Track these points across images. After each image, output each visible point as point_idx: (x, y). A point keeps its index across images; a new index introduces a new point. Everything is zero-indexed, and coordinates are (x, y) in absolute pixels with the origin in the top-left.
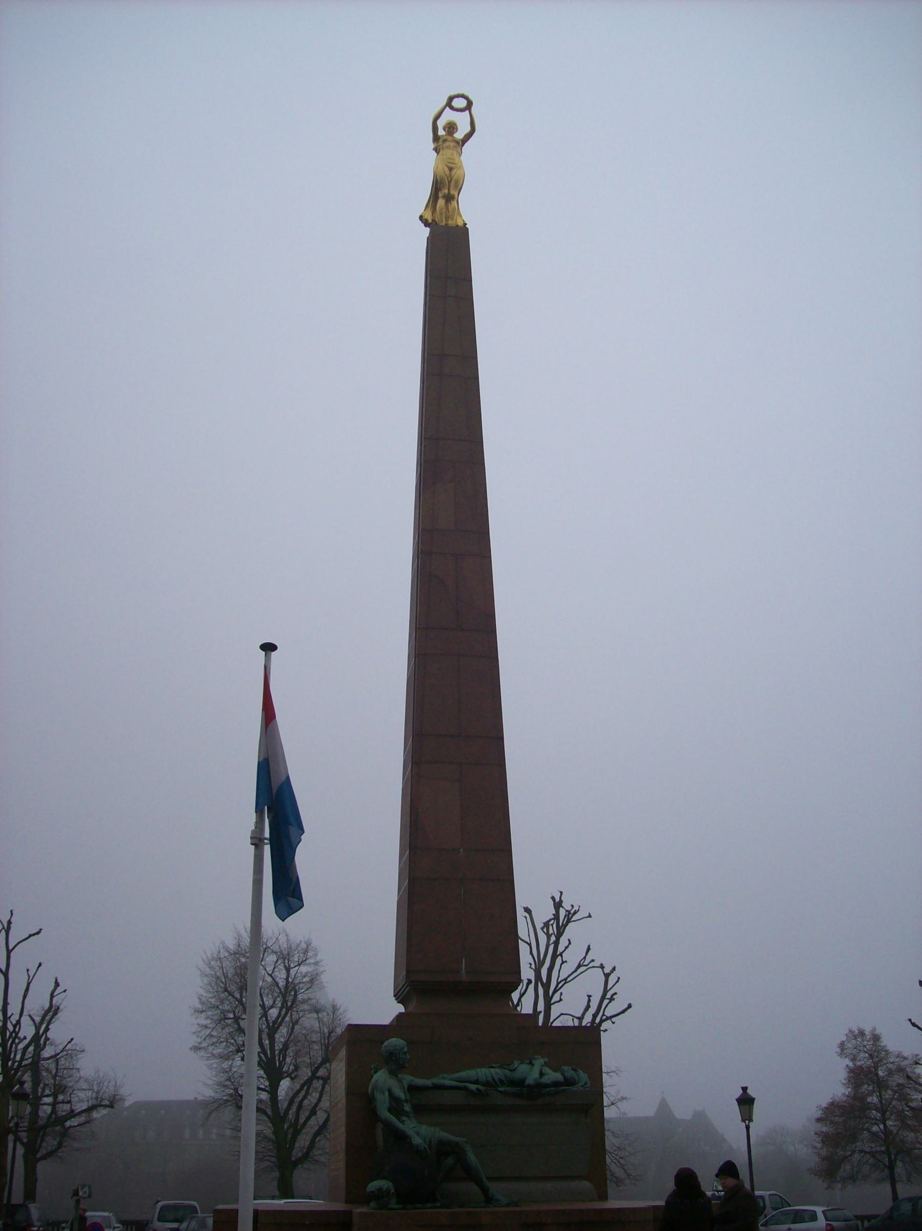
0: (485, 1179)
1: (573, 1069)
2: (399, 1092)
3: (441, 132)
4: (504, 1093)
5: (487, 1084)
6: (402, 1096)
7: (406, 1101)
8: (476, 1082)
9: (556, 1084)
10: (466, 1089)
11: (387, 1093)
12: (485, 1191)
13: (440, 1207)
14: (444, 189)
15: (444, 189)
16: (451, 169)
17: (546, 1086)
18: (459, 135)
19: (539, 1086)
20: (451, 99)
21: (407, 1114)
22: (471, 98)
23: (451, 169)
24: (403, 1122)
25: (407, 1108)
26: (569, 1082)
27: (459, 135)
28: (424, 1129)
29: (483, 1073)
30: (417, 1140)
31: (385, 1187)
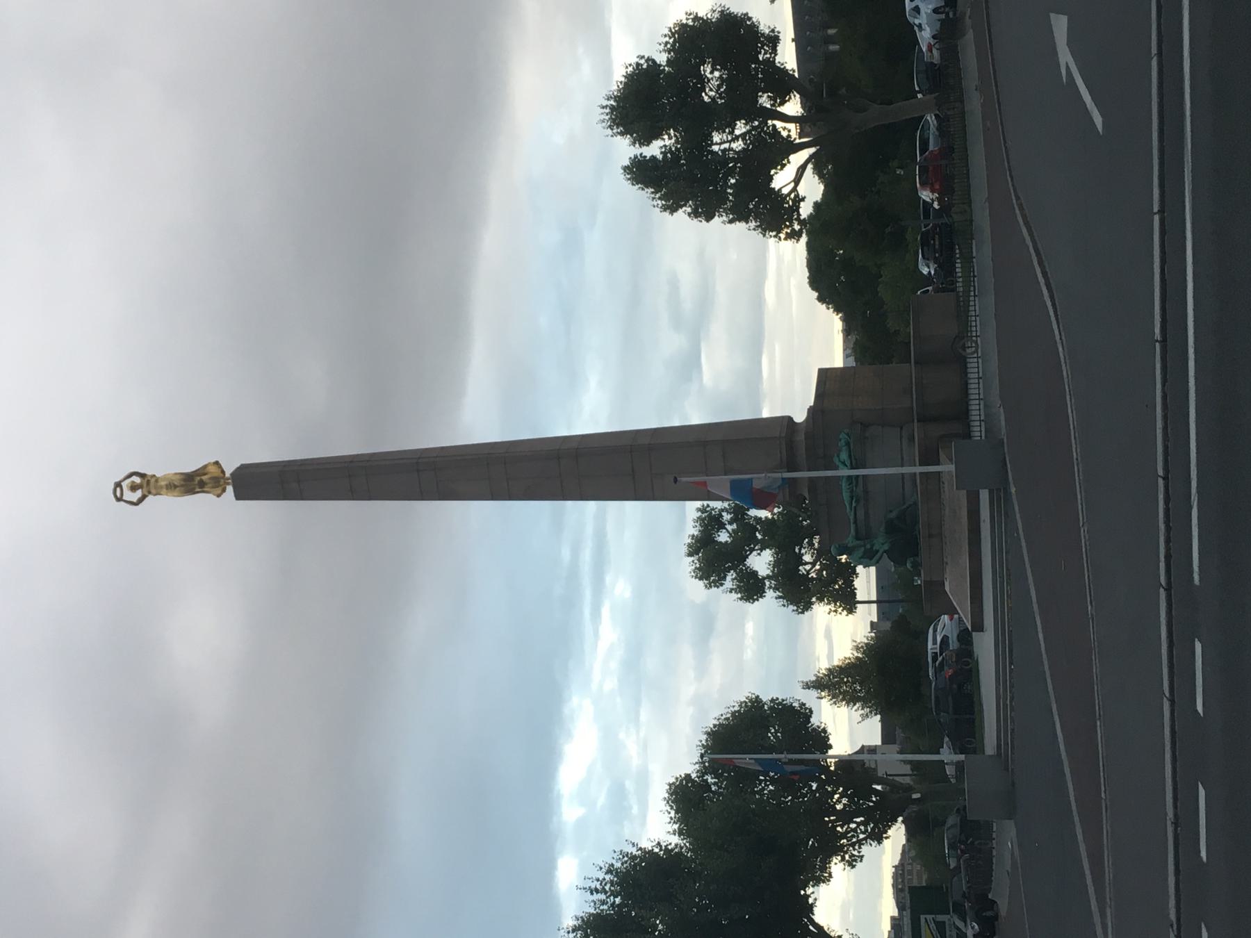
3: (139, 493)
5: (852, 491)
8: (852, 498)
9: (850, 456)
14: (191, 483)
15: (191, 483)
16: (176, 487)
18: (137, 480)
20: (119, 499)
21: (872, 546)
22: (112, 487)
23: (176, 487)
25: (868, 546)
26: (848, 444)
27: (137, 480)
28: (881, 540)
29: (846, 495)
30: (886, 547)
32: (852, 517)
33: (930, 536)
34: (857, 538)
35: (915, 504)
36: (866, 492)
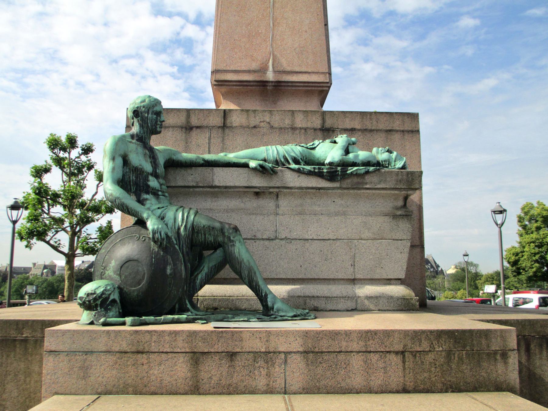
0: (261, 283)
1: (388, 151)
2: (138, 159)
4: (298, 171)
6: (148, 167)
7: (156, 175)
8: (265, 160)
10: (246, 165)
11: (119, 161)
12: (262, 297)
13: (188, 321)
17: (354, 164)
19: (344, 164)
21: (155, 193)
24: (141, 202)
25: (153, 183)
29: (272, 151)
31: (99, 291)
32: (221, 156)
33: (197, 358)
34: (173, 164)
35: (267, 312)
36: (275, 194)
